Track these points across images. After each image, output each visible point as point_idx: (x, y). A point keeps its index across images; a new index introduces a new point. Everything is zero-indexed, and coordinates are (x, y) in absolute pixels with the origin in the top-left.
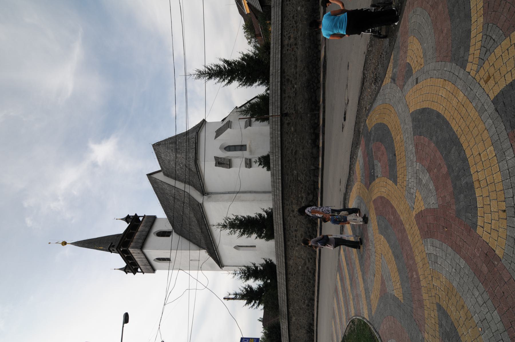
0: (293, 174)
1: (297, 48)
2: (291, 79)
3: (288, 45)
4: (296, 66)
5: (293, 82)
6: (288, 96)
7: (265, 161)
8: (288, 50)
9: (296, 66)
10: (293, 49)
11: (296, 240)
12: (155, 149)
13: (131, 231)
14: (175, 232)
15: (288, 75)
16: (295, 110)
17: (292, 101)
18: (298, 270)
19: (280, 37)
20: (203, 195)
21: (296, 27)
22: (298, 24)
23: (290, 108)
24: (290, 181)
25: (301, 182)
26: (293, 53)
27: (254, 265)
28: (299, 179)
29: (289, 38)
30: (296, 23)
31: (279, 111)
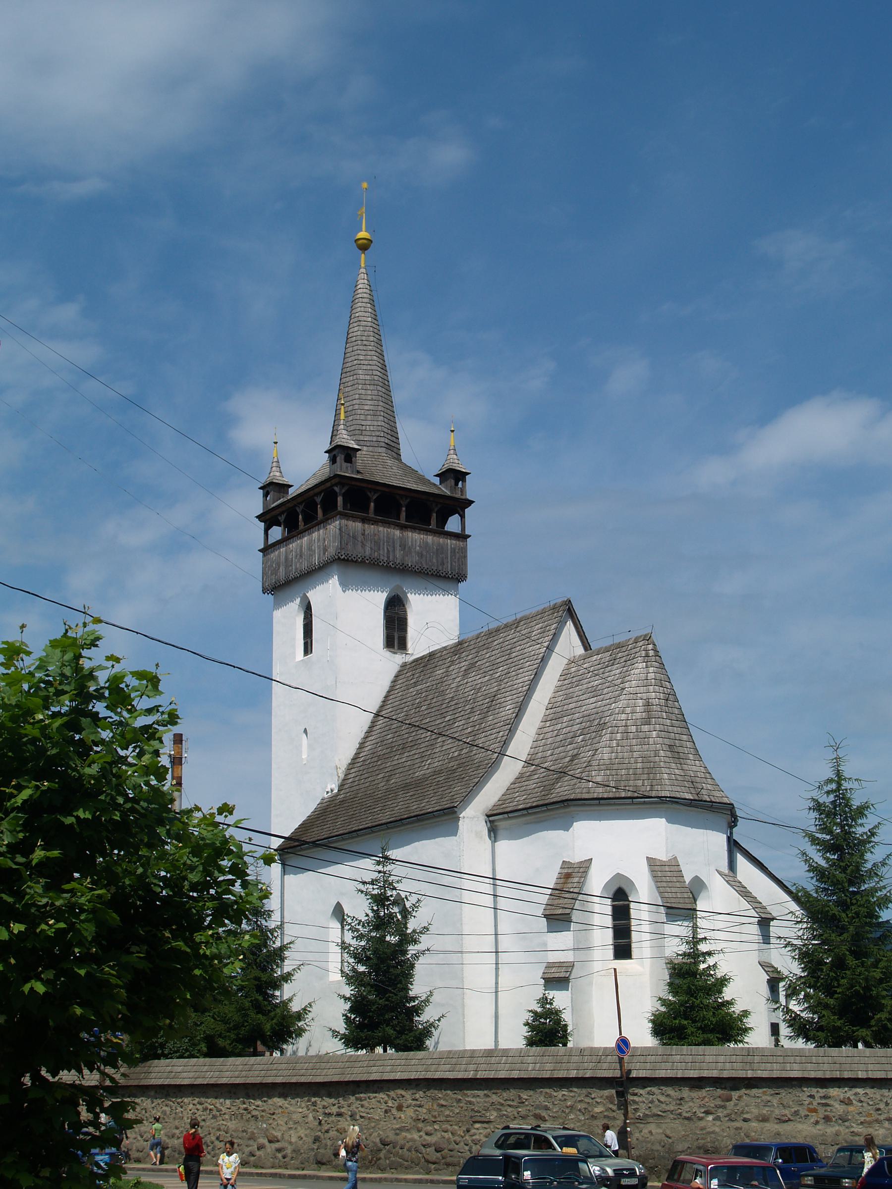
0: (487, 1110)
1: (817, 1123)
3: (825, 1097)
4: (764, 1119)
5: (721, 1113)
7: (547, 1030)
8: (812, 1096)
10: (815, 1111)
11: (330, 1114)
13: (404, 502)
14: (404, 665)
16: (646, 1116)
17: (672, 1108)
18: (256, 1118)
19: (846, 1075)
20: (488, 816)
21: (877, 1121)
22: (886, 1124)
23: (652, 1102)
24: (470, 1103)
25: (468, 1131)
26: (803, 1113)
27: (287, 977)
28: (477, 1125)
29: (847, 1102)
31: (642, 1074)
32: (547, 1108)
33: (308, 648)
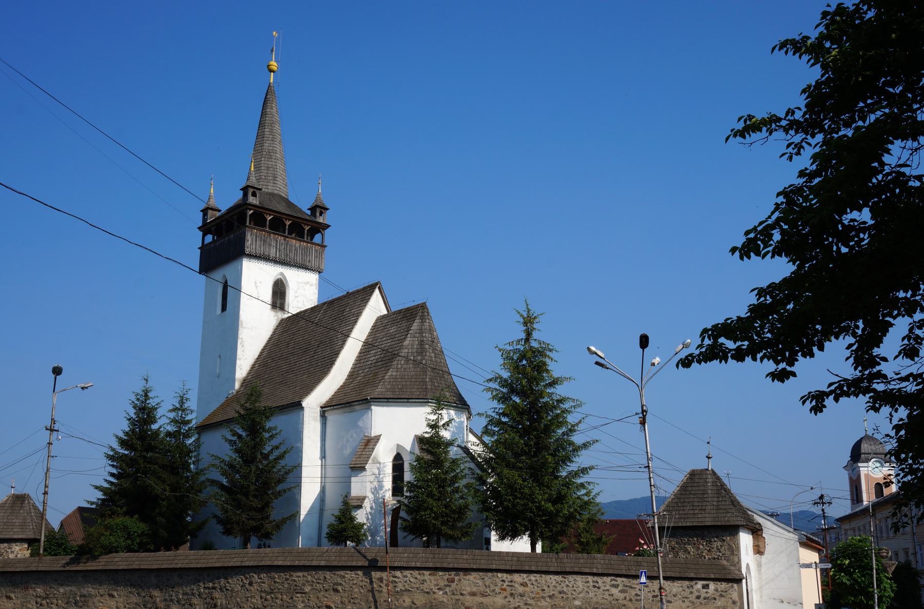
0: (304, 585)
1: (506, 597)
2: (453, 585)
4: (473, 594)
5: (447, 589)
6: (424, 581)
8: (503, 581)
9: (473, 594)
10: (505, 590)
12: (417, 306)
15: (460, 580)
21: (543, 597)
22: (548, 599)
24: (295, 581)
26: (497, 590)
28: (298, 595)
29: (524, 585)
30: (550, 597)
32: (341, 584)
33: (224, 308)
